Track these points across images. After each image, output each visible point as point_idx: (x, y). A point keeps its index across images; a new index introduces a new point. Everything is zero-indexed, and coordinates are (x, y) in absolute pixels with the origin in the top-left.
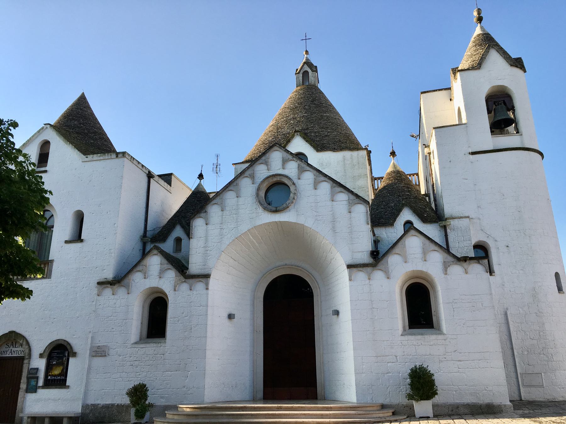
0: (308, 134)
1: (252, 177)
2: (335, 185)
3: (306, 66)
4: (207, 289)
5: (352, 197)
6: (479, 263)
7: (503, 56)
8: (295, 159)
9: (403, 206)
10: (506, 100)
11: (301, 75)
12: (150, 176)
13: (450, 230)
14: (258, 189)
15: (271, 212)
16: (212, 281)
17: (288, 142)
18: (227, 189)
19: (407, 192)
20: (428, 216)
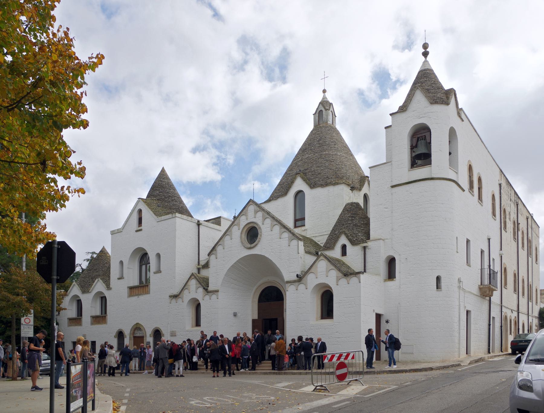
1: (238, 225)
2: (282, 227)
5: (291, 235)
6: (356, 276)
9: (341, 233)
11: (317, 115)
14: (241, 233)
19: (350, 221)
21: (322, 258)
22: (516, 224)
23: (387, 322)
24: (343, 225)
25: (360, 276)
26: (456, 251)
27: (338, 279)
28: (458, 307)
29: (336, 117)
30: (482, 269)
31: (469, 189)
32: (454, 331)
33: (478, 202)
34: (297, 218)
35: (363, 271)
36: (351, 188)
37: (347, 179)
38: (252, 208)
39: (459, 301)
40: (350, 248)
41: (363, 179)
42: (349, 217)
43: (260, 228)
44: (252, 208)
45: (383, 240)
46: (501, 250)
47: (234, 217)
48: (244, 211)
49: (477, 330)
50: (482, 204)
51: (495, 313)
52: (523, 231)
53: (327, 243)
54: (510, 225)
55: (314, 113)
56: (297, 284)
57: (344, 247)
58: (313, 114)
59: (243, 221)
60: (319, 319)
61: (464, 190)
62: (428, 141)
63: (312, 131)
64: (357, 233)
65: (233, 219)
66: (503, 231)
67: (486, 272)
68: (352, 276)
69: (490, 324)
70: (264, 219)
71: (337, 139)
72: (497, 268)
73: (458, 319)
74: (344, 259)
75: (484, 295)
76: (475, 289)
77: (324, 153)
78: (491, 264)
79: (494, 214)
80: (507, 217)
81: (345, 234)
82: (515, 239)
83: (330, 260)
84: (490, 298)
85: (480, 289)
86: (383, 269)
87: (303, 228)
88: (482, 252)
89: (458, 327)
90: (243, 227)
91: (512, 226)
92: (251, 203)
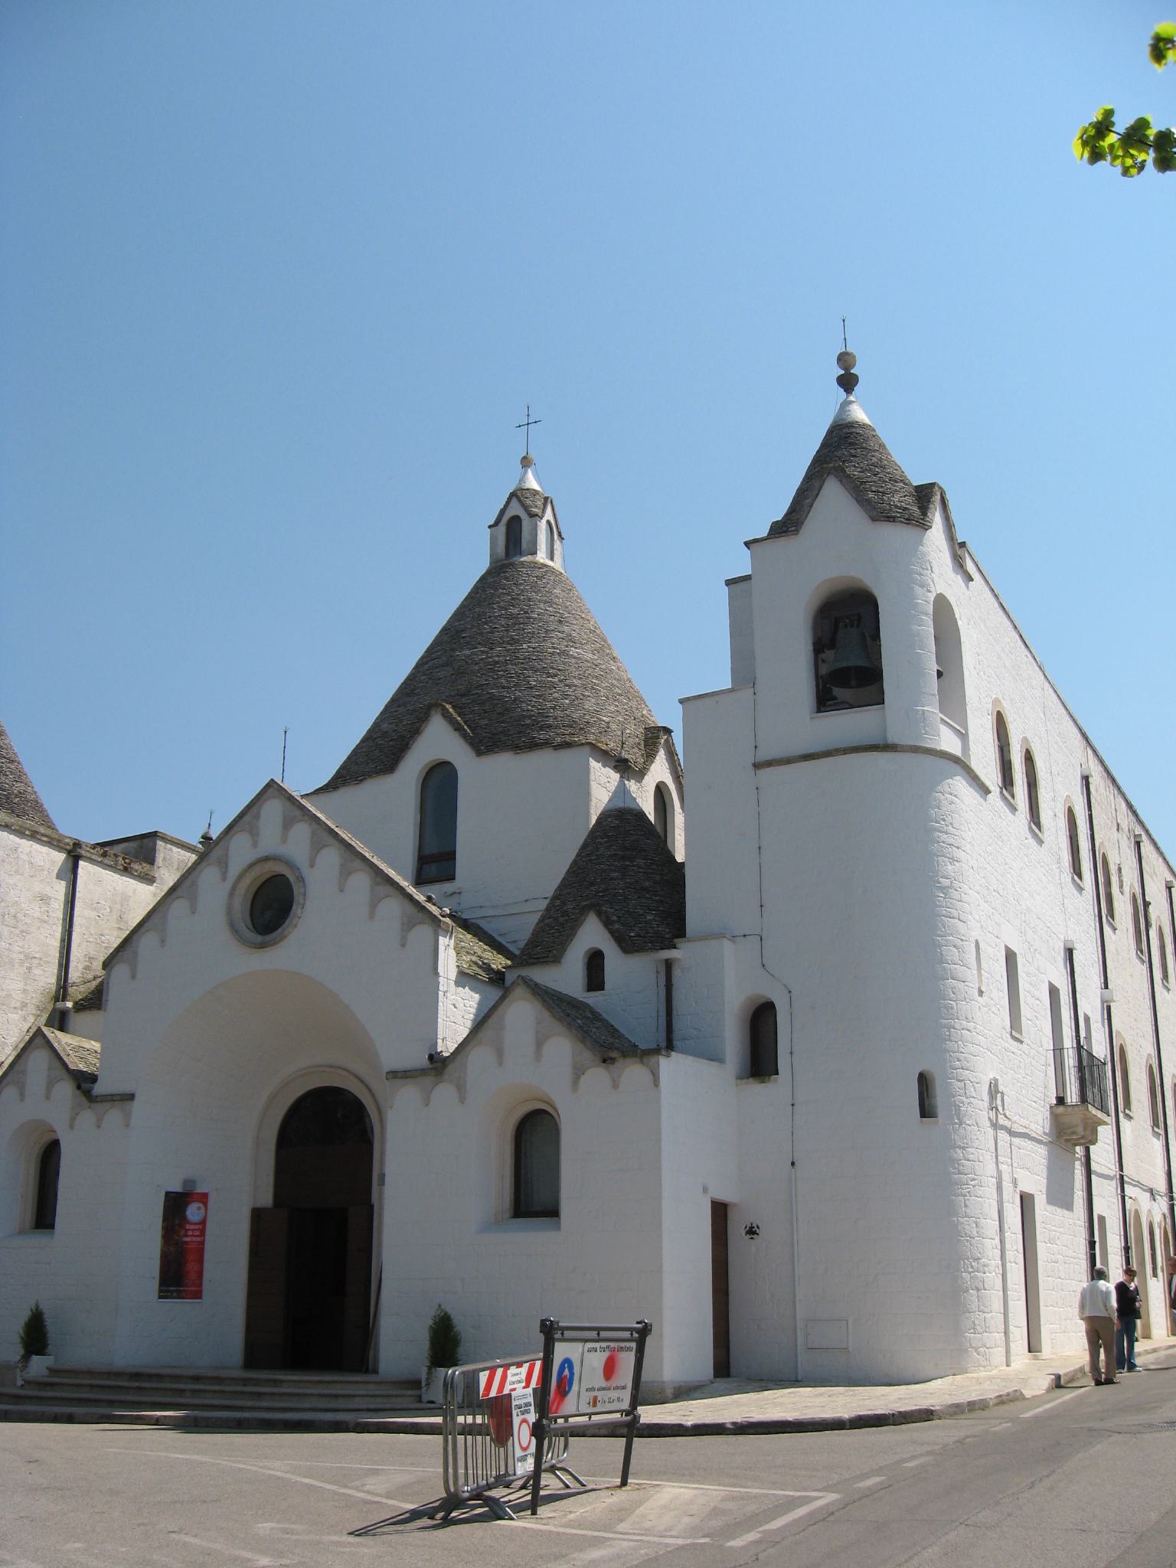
1: (223, 864)
2: (379, 879)
3: (514, 502)
4: (127, 1125)
5: (411, 909)
6: (642, 1062)
7: (854, 496)
9: (583, 911)
11: (502, 529)
14: (231, 894)
15: (256, 948)
16: (136, 1104)
17: (415, 734)
18: (174, 895)
21: (520, 991)
22: (1141, 908)
23: (752, 1231)
24: (592, 884)
26: (977, 986)
27: (578, 1073)
28: (994, 1180)
29: (563, 539)
30: (1058, 1050)
31: (1001, 789)
32: (986, 1269)
33: (1030, 828)
34: (427, 851)
35: (663, 1044)
36: (617, 761)
37: (601, 733)
38: (273, 809)
39: (994, 1160)
40: (616, 964)
41: (654, 737)
42: (611, 856)
43: (301, 879)
44: (273, 809)
46: (1106, 987)
47: (203, 837)
48: (247, 818)
49: (1057, 1262)
50: (1040, 835)
51: (1106, 1204)
52: (1160, 928)
53: (535, 941)
54: (1123, 908)
55: (492, 522)
56: (428, 1080)
57: (595, 962)
58: (490, 527)
59: (241, 853)
60: (508, 1214)
61: (985, 791)
63: (483, 579)
64: (641, 912)
65: (200, 842)
66: (1107, 929)
67: (1070, 1060)
69: (1095, 1242)
71: (567, 607)
72: (1100, 1050)
73: (997, 1223)
74: (593, 999)
75: (1067, 1141)
76: (1038, 1121)
77: (525, 646)
78: (1083, 1034)
79: (1077, 871)
80: (1114, 879)
81: (599, 914)
82: (1142, 952)
83: (556, 1003)
84: (1087, 1150)
85: (1055, 1118)
86: (732, 1039)
87: (447, 887)
88: (1054, 992)
89: (998, 1252)
91: (1130, 909)
92: (271, 790)
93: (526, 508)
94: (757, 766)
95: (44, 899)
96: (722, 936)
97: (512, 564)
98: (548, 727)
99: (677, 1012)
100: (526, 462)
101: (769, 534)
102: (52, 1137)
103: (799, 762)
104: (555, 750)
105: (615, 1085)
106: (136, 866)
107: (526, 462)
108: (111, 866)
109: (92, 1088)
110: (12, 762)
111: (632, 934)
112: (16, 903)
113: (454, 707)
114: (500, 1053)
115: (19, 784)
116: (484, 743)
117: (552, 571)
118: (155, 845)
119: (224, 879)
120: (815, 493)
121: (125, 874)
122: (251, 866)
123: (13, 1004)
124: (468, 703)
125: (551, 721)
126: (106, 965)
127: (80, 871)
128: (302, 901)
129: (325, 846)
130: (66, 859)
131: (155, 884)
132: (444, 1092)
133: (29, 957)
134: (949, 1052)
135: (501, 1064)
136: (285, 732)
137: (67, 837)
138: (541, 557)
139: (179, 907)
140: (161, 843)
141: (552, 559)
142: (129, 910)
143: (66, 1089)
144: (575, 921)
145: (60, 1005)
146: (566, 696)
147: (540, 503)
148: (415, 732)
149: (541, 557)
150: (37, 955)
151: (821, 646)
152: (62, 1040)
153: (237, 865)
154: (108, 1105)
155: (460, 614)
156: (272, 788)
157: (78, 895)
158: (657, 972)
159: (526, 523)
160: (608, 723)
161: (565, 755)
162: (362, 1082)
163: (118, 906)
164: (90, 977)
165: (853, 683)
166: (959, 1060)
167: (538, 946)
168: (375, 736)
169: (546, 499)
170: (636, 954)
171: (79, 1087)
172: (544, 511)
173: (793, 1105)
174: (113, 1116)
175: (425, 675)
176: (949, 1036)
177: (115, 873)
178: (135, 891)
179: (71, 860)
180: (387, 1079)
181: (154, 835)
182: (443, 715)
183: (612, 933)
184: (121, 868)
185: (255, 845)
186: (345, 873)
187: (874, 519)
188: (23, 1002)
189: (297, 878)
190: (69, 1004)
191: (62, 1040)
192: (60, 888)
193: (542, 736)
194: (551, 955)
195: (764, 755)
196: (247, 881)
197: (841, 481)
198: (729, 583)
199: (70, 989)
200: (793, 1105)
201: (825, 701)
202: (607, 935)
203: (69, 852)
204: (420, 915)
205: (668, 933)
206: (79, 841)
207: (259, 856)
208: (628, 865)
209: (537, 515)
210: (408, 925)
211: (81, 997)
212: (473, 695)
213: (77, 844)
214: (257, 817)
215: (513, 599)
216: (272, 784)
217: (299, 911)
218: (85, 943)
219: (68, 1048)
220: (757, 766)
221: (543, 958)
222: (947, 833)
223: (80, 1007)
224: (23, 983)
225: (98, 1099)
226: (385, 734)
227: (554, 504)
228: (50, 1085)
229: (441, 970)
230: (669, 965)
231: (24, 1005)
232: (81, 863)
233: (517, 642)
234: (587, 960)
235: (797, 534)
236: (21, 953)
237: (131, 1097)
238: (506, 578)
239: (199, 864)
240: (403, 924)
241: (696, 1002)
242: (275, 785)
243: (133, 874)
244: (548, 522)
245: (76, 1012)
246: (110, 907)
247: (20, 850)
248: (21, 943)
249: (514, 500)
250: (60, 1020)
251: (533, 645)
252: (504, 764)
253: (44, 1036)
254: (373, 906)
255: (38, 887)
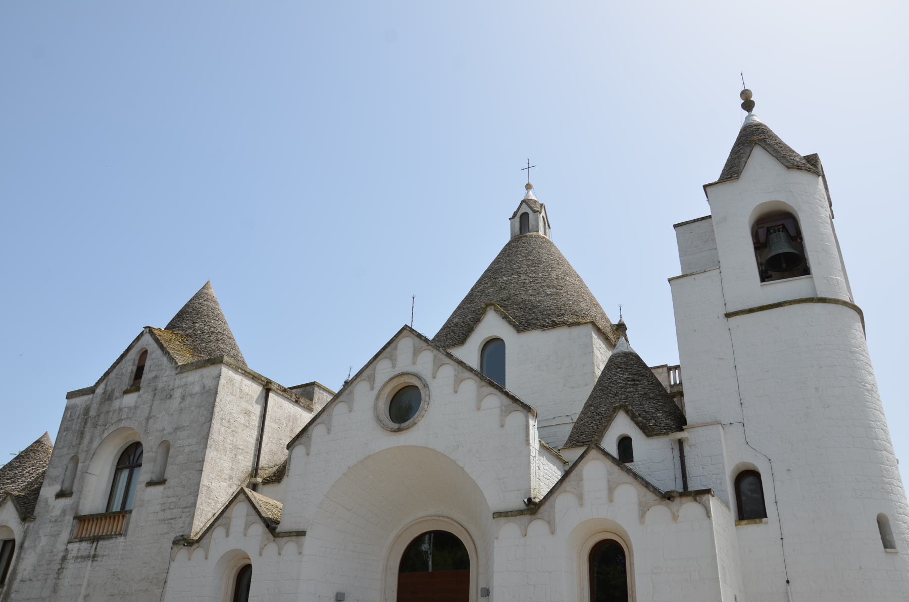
0: (508, 307)
1: (371, 379)
2: (483, 383)
3: (524, 205)
6: (696, 500)
7: (774, 155)
8: (430, 347)
9: (616, 410)
10: (788, 224)
11: (517, 219)
12: (268, 387)
13: (690, 446)
14: (377, 398)
16: (307, 540)
17: (477, 322)
18: (338, 400)
19: (630, 388)
20: (656, 426)
24: (616, 395)
25: (709, 500)
27: (643, 510)
29: (550, 228)
38: (406, 344)
42: (624, 378)
43: (426, 386)
44: (406, 344)
45: (723, 426)
48: (388, 350)
55: (511, 217)
56: (525, 518)
57: (625, 444)
58: (510, 219)
59: (384, 371)
62: (792, 233)
64: (654, 411)
68: (684, 499)
70: (438, 365)
71: (560, 258)
77: (540, 274)
81: (627, 412)
90: (381, 385)
92: (405, 332)
93: (531, 208)
94: (728, 315)
95: (247, 413)
96: (718, 423)
97: (526, 236)
98: (562, 315)
99: (689, 475)
100: (528, 187)
101: (719, 180)
102: (246, 562)
103: (758, 311)
104: (569, 327)
105: (675, 517)
106: (302, 400)
107: (528, 187)
108: (288, 398)
109: (276, 528)
110: (230, 338)
111: (651, 424)
112: (231, 413)
113: (500, 306)
114: (580, 498)
115: (234, 351)
116: (523, 325)
117: (546, 240)
118: (314, 389)
119: (372, 389)
120: (748, 155)
121: (296, 404)
122: (391, 379)
123: (224, 476)
124: (510, 305)
125: (563, 312)
126: (289, 446)
127: (270, 399)
128: (427, 400)
129: (443, 364)
130: (262, 392)
131: (313, 413)
132: (537, 526)
133: (236, 447)
134: (894, 501)
135: (581, 505)
136: (413, 298)
137: (263, 377)
138: (541, 233)
139: (340, 408)
140: (317, 389)
141: (546, 235)
142: (298, 426)
143: (259, 529)
144: (609, 417)
145: (253, 480)
146: (569, 300)
147: (539, 206)
148: (478, 320)
149: (541, 233)
150: (241, 447)
151: (760, 246)
152: (256, 496)
153: (381, 379)
154: (288, 539)
155: (497, 261)
156: (407, 330)
157: (267, 413)
158: (672, 449)
159: (532, 216)
160: (595, 316)
161: (576, 330)
162: (462, 526)
163: (291, 423)
164: (272, 464)
165: (784, 266)
166: (901, 508)
167: (582, 435)
168: (450, 326)
169: (542, 205)
170: (656, 437)
171: (268, 526)
172: (541, 210)
173: (782, 539)
174: (290, 546)
175: (478, 292)
176: (891, 490)
177: (290, 403)
178: (301, 416)
179: (265, 391)
180: (494, 518)
181: (313, 384)
182: (495, 310)
183: (637, 423)
184: (294, 400)
185: (394, 367)
186: (458, 381)
187: (789, 168)
188: (230, 476)
189: (424, 385)
190: (259, 480)
191: (256, 496)
192: (257, 409)
193: (559, 320)
194: (593, 439)
195: (731, 309)
196: (388, 389)
197: (764, 148)
198: (675, 226)
199: (259, 471)
200: (782, 539)
201: (765, 277)
202: (633, 425)
203: (264, 386)
204: (515, 405)
205: (673, 425)
206: (271, 380)
207: (396, 373)
208: (638, 384)
209: (538, 211)
210: (505, 412)
211: (265, 476)
212: (512, 300)
213: (269, 382)
214: (396, 348)
215: (529, 252)
216: (405, 328)
217: (426, 406)
218: (270, 443)
219: (260, 502)
220: (728, 315)
221: (588, 442)
222: (863, 356)
223: (266, 482)
224: (231, 464)
225: (280, 535)
226: (456, 324)
227: (545, 207)
228: (247, 526)
229: (531, 441)
230: (680, 443)
231: (231, 478)
232: (271, 394)
233: (535, 272)
234: (618, 443)
235: (738, 179)
236: (231, 444)
237: (301, 534)
238: (524, 243)
239: (355, 380)
240: (502, 411)
241: (703, 468)
242: (407, 328)
243: (300, 405)
244: (543, 217)
245: (263, 485)
246: (286, 423)
247: (234, 381)
248: (231, 439)
249: (524, 204)
250: (254, 487)
251: (546, 274)
252: (535, 337)
253: (245, 493)
254: (480, 399)
255: (244, 405)
